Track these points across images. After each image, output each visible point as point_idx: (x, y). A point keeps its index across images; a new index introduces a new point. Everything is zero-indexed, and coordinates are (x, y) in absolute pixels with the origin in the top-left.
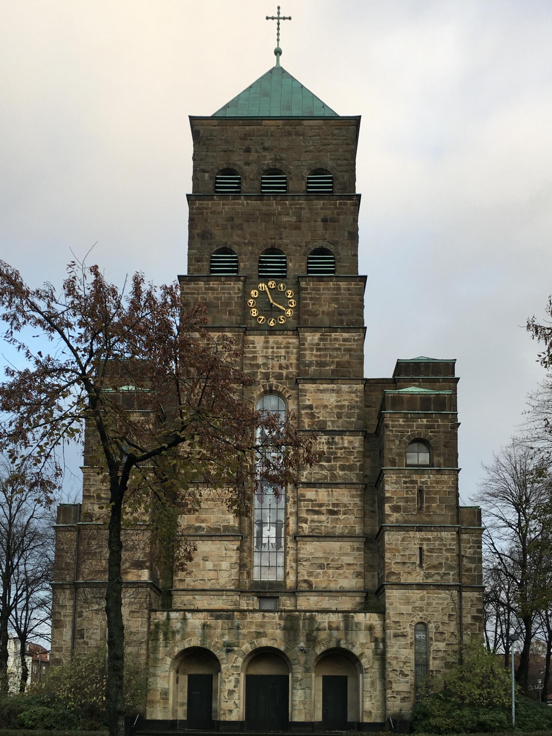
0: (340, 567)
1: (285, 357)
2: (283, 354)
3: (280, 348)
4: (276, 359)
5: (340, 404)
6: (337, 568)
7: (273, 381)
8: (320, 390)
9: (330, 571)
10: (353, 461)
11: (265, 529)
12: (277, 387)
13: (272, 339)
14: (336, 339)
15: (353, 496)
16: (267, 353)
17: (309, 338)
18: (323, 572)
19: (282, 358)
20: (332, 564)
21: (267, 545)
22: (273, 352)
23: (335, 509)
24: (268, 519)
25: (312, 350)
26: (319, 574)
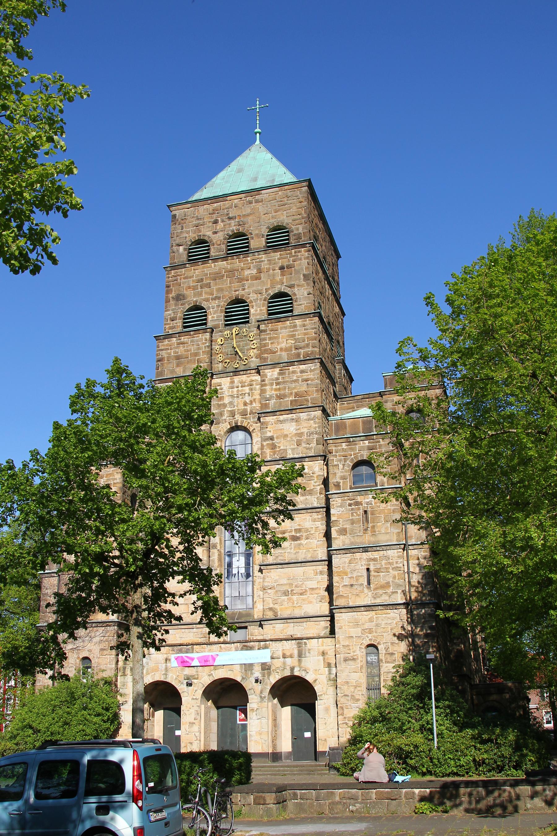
0: (304, 592)
1: (249, 394)
2: (247, 391)
3: (245, 386)
4: (240, 397)
5: (299, 432)
6: (301, 594)
7: (238, 417)
8: (280, 421)
9: (295, 597)
10: (314, 486)
11: (235, 559)
12: (242, 422)
13: (237, 379)
14: (294, 372)
15: (314, 520)
16: (232, 392)
17: (269, 374)
18: (288, 599)
19: (247, 395)
20: (296, 590)
21: (237, 575)
22: (238, 391)
23: (298, 535)
24: (237, 549)
25: (272, 384)
26: (284, 600)
